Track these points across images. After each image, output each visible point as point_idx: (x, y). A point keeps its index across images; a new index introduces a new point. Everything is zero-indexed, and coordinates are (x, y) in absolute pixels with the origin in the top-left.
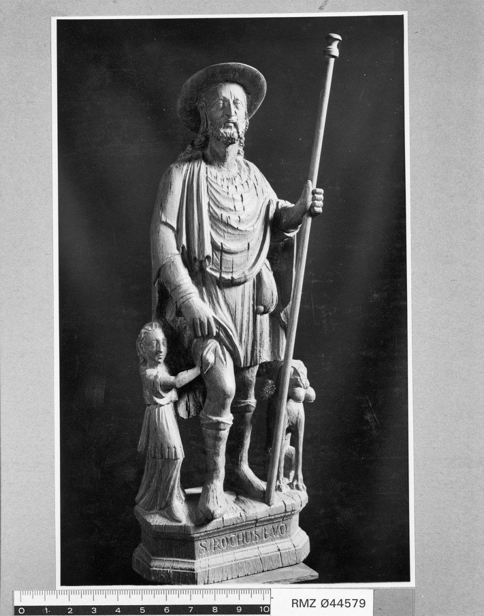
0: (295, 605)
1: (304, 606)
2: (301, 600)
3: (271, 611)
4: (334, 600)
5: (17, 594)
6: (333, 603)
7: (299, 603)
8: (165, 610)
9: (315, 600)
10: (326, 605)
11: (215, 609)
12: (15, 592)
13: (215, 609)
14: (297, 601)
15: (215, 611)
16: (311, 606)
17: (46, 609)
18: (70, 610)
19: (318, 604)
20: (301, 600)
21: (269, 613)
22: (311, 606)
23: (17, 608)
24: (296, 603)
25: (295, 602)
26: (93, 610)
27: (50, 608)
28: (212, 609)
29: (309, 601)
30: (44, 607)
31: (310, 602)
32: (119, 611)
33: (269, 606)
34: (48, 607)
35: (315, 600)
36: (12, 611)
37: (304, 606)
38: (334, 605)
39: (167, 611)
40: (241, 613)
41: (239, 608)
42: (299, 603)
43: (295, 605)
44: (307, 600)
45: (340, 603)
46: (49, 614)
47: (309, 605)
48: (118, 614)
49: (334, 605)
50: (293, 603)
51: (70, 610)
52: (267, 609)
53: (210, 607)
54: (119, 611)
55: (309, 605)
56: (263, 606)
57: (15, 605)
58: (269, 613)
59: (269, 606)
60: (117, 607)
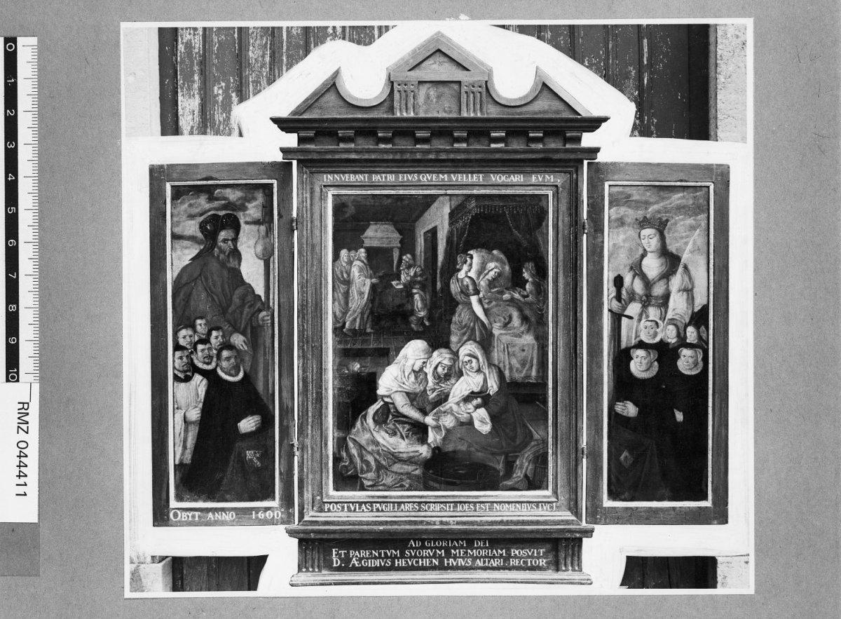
0: (21, 406)
1: (19, 418)
2: (28, 414)
3: (11, 383)
4: (26, 456)
5: (33, 41)
6: (22, 454)
7: (23, 411)
8: (12, 241)
9: (27, 433)
10: (20, 445)
11: (13, 308)
12: (36, 38)
13: (13, 308)
14: (27, 409)
15: (11, 308)
16: (19, 427)
17: (13, 81)
18: (12, 112)
19: (22, 436)
20: (28, 414)
21: (8, 381)
22: (19, 427)
23: (14, 40)
24: (24, 408)
25: (26, 406)
26: (11, 143)
27: (15, 84)
28: (13, 304)
29: (26, 425)
30: (16, 77)
31: (24, 427)
32: (10, 179)
33: (18, 381)
34: (16, 83)
35: (27, 433)
36: (9, 35)
37: (19, 418)
38: (20, 457)
39: (11, 243)
40: (7, 343)
41: (14, 340)
42: (23, 411)
43: (21, 406)
44: (27, 423)
45: (21, 474)
46: (6, 84)
47: (20, 425)
48: (7, 176)
49: (20, 457)
50: (23, 403)
51: (12, 113)
52: (13, 377)
53: (16, 302)
54: (10, 179)
55: (20, 425)
56: (18, 373)
57: (18, 38)
58: (8, 381)
59: (18, 381)
60: (16, 174)
